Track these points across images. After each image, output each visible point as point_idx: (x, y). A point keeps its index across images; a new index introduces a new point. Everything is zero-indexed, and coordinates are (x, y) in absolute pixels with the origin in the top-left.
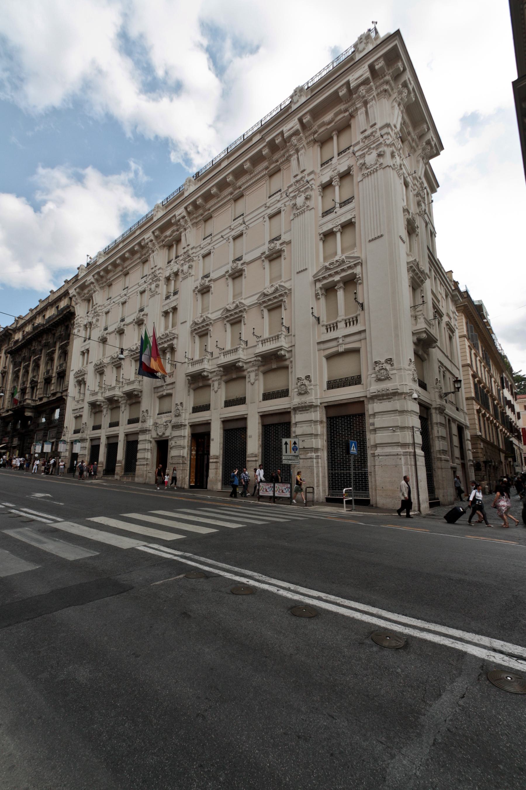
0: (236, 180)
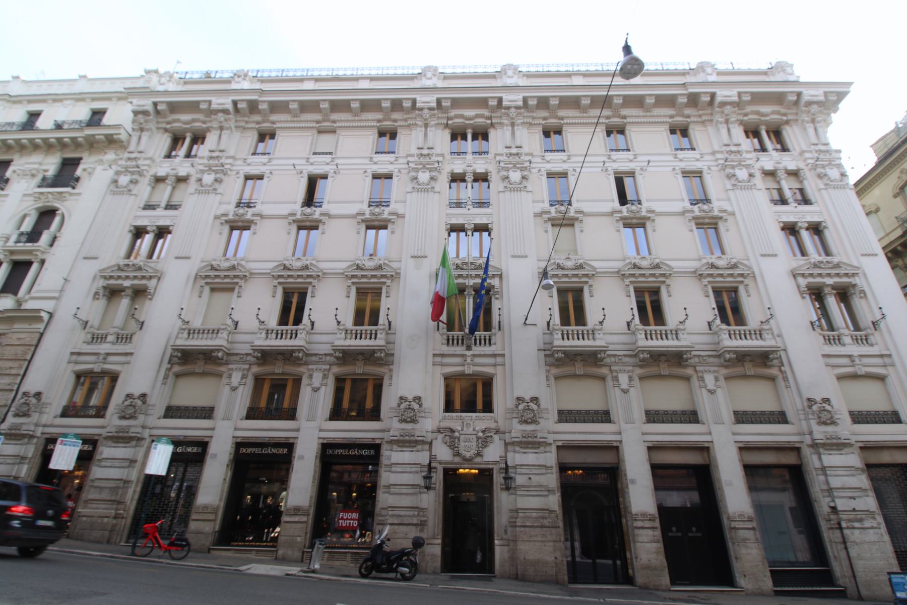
0: (331, 112)
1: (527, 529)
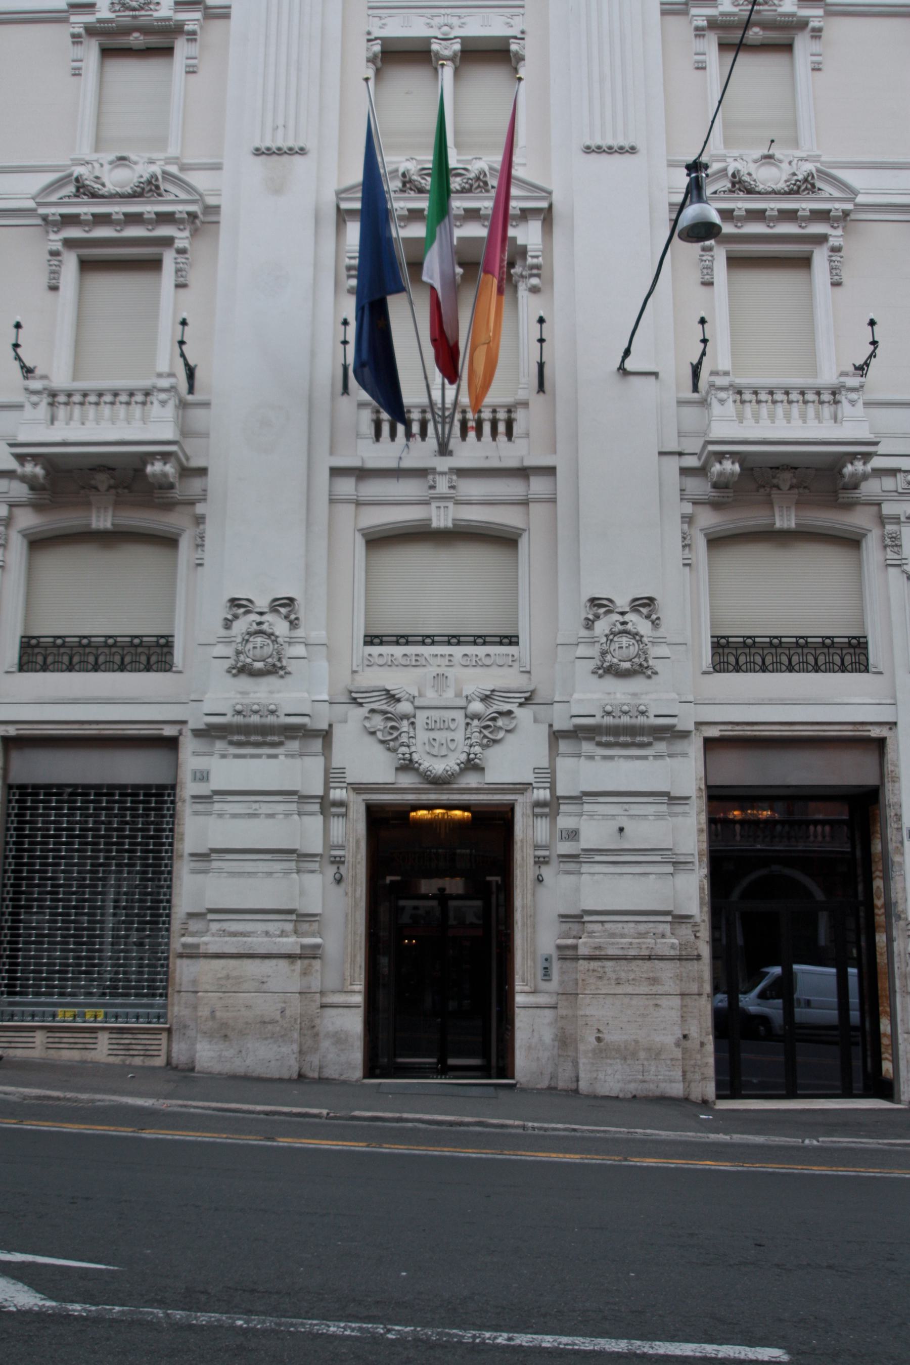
1: (609, 964)
